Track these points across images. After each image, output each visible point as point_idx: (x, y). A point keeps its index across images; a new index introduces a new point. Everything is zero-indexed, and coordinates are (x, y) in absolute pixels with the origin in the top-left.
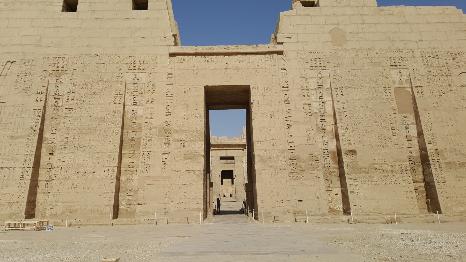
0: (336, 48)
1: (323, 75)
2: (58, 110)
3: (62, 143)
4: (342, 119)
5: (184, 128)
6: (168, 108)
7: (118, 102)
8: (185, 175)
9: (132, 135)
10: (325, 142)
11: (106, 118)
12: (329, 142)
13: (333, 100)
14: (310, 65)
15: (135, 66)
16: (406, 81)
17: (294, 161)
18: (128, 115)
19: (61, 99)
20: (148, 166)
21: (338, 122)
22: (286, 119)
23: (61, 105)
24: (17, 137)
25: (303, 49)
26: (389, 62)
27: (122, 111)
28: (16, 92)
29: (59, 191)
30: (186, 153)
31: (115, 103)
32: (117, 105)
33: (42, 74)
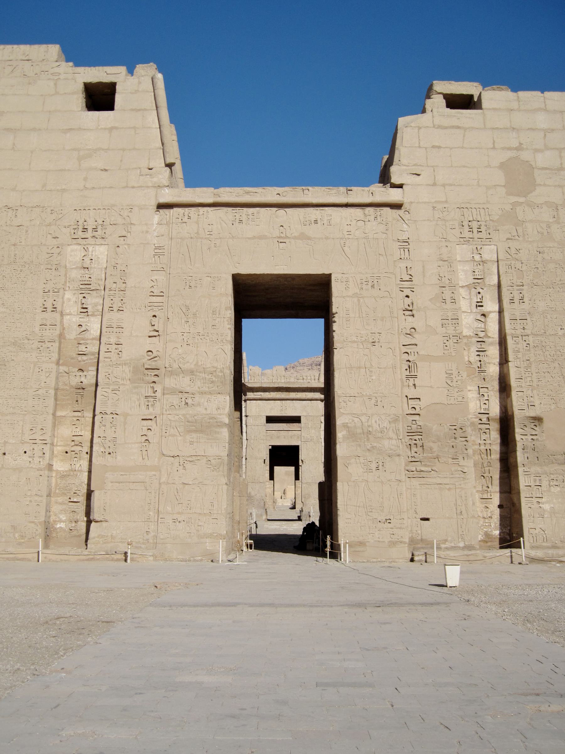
1: (486, 256)
4: (518, 351)
7: (50, 308)
8: (188, 465)
9: (78, 377)
10: (483, 400)
11: (26, 341)
13: (501, 312)
14: (459, 235)
15: (85, 230)
17: (416, 438)
18: (72, 335)
20: (111, 445)
21: (511, 357)
22: (405, 349)
25: (444, 200)
27: (58, 327)
30: (190, 419)
31: (45, 310)
32: (48, 315)
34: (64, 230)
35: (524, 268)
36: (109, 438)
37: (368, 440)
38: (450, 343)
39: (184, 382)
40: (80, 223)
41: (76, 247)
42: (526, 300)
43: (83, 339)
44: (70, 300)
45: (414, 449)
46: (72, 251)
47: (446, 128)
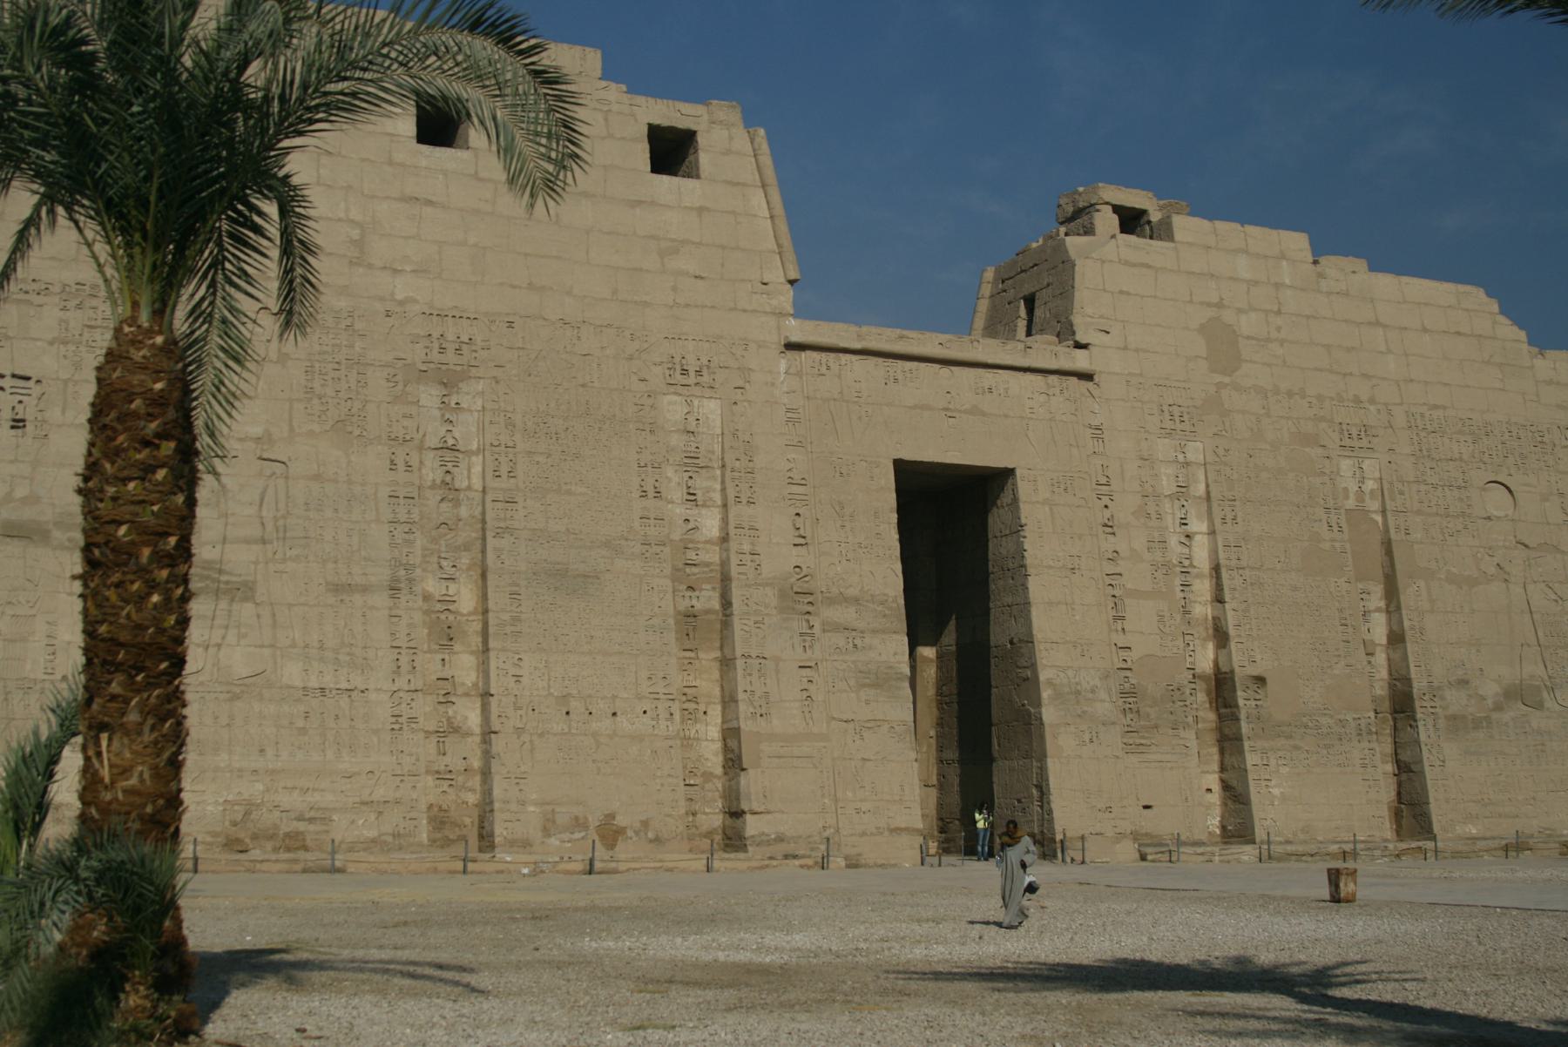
0: (1218, 378)
1: (1191, 457)
2: (457, 503)
3: (506, 617)
5: (852, 592)
6: (799, 522)
7: (651, 494)
12: (1198, 649)
15: (685, 372)
16: (1372, 491)
19: (463, 465)
23: (465, 484)
24: (349, 588)
26: (1336, 436)
28: (316, 428)
29: (523, 769)
31: (644, 494)
32: (650, 503)
33: (392, 371)
34: (658, 370)
35: (1235, 476)
36: (758, 694)
37: (1078, 702)
38: (1159, 575)
39: (846, 614)
40: (677, 360)
41: (675, 398)
42: (1239, 520)
43: (692, 541)
44: (673, 479)
45: (1129, 716)
46: (670, 403)
47: (1134, 265)
